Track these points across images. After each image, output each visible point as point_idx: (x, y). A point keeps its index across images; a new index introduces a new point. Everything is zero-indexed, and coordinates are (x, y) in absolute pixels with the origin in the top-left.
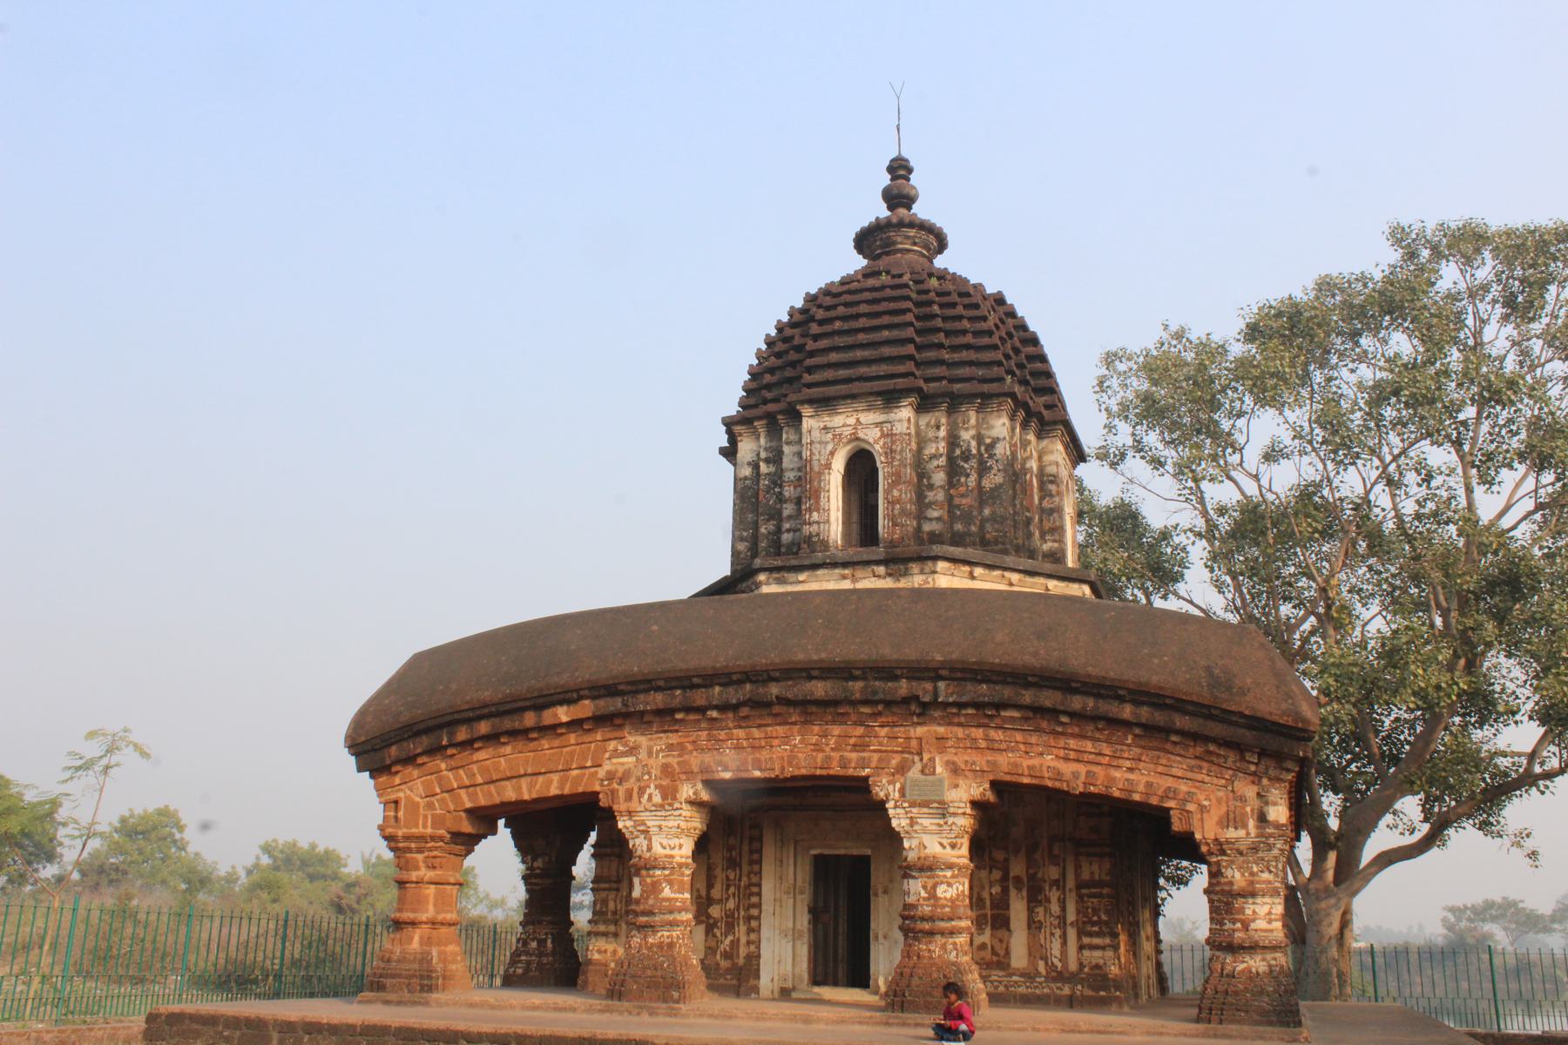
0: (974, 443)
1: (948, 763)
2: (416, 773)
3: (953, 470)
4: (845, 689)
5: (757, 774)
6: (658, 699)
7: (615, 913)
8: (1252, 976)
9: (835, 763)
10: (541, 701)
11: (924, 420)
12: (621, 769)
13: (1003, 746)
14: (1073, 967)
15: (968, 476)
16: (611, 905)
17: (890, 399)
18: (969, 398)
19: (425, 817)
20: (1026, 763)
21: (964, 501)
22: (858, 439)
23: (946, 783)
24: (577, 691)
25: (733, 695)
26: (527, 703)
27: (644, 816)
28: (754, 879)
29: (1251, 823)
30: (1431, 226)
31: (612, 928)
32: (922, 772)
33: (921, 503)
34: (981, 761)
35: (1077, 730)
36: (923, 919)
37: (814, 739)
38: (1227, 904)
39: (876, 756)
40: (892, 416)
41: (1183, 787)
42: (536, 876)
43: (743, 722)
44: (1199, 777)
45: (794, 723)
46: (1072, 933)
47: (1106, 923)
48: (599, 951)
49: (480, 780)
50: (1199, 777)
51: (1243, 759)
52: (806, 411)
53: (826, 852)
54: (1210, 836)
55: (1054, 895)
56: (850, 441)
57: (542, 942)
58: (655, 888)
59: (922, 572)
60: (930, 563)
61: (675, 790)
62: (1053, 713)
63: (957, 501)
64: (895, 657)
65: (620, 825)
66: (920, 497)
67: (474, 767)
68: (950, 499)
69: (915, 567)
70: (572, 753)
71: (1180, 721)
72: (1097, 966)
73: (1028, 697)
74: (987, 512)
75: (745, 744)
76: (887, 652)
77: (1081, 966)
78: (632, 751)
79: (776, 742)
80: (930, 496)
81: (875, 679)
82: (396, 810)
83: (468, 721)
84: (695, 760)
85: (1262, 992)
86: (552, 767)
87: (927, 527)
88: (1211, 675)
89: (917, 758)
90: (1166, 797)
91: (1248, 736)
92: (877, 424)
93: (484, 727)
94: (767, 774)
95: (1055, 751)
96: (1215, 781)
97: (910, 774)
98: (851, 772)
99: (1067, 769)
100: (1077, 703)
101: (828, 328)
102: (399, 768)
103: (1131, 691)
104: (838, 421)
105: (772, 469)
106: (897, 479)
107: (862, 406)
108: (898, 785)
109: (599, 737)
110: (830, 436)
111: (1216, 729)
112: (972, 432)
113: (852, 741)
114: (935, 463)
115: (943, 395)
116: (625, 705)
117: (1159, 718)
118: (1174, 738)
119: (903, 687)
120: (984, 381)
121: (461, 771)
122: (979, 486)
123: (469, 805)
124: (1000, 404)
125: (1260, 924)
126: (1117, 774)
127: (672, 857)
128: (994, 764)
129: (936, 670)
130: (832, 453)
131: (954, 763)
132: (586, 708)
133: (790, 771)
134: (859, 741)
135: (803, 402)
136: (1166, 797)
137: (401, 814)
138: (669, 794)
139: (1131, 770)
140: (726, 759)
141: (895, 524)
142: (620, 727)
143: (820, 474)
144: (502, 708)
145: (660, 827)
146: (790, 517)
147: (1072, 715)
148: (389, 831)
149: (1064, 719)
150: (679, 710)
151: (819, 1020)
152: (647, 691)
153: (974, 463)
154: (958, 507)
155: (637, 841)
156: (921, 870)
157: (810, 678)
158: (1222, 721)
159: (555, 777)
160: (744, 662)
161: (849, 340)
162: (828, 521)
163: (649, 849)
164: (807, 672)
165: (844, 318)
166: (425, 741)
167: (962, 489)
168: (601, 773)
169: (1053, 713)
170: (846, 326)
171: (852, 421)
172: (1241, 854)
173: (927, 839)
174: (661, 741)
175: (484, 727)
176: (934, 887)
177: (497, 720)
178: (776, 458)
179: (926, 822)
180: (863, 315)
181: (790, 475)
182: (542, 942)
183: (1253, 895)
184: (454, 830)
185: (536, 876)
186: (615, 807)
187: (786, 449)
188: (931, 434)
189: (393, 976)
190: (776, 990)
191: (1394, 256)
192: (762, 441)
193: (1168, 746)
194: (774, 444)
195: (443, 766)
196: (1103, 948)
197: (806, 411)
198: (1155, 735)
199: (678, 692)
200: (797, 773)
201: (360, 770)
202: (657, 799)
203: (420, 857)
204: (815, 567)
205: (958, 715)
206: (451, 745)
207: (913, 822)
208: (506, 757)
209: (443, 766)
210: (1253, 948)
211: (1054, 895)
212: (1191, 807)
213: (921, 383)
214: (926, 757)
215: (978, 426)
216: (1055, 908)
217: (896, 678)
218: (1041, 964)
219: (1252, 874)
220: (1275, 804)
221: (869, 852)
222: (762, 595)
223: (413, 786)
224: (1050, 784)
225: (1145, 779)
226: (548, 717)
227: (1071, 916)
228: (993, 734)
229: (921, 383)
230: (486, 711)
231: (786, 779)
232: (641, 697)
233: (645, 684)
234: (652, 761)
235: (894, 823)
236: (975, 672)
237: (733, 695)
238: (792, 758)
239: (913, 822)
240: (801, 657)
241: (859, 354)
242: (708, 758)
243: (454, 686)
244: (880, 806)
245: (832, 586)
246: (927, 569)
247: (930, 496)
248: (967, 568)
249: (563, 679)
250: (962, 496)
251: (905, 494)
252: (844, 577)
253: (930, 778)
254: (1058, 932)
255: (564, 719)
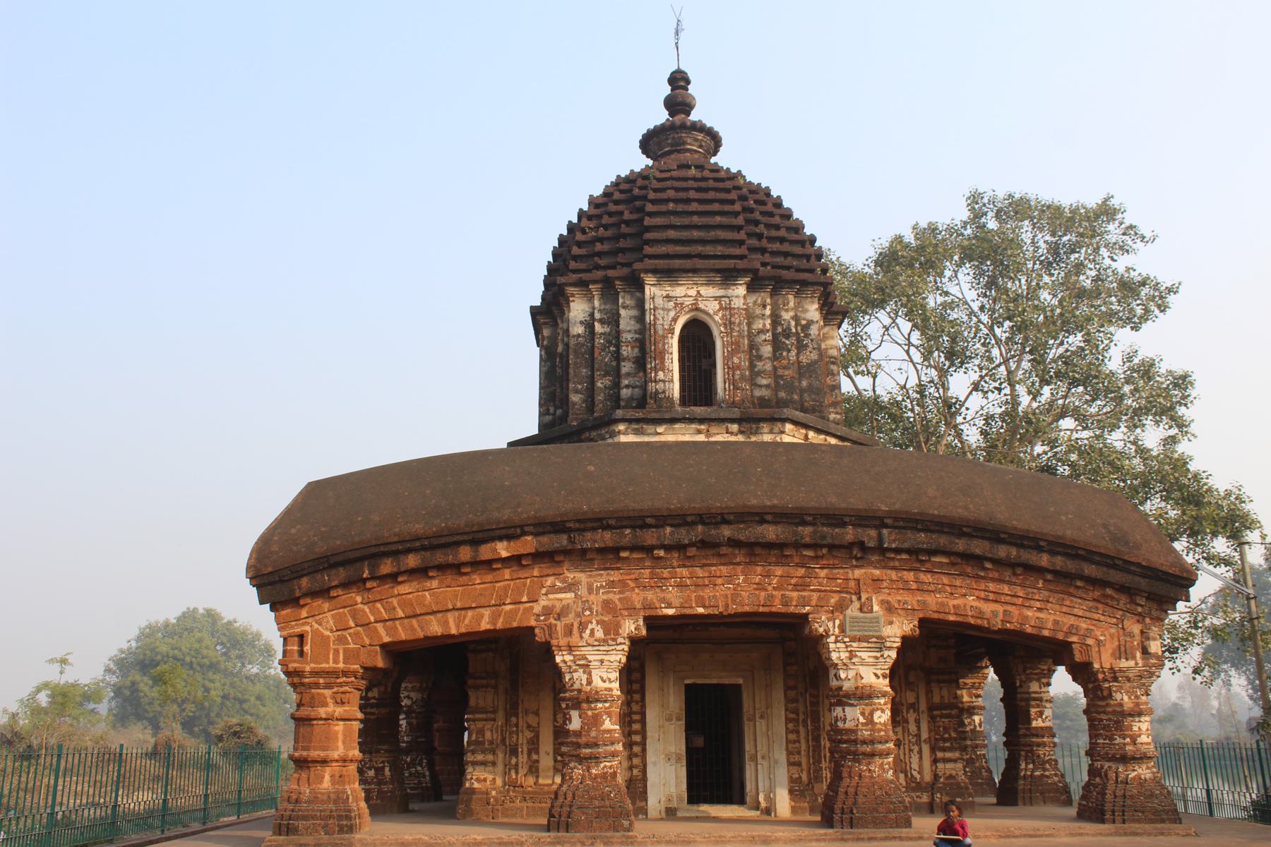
0: (793, 323)
1: (882, 602)
2: (326, 606)
3: (777, 344)
4: (795, 533)
5: (701, 610)
6: (607, 538)
7: (491, 742)
8: (1141, 782)
9: (777, 602)
10: (480, 535)
11: (751, 300)
12: (558, 606)
13: (932, 587)
14: (928, 777)
15: (789, 351)
16: (488, 735)
17: (728, 277)
18: (791, 283)
19: (337, 651)
20: (952, 603)
21: (787, 373)
22: (697, 309)
23: (882, 620)
24: (521, 527)
25: (684, 535)
26: (465, 537)
27: (586, 651)
28: (635, 708)
29: (1138, 655)
30: (1001, 194)
31: (490, 757)
32: (861, 610)
33: (755, 374)
34: (912, 600)
35: (996, 575)
36: (864, 742)
37: (757, 579)
38: (1117, 722)
39: (815, 596)
40: (730, 292)
41: (1084, 626)
42: (372, 706)
43: (687, 561)
44: (1096, 616)
45: (739, 564)
46: (926, 749)
47: (955, 739)
48: (478, 780)
49: (401, 614)
50: (1096, 616)
51: (1133, 602)
52: (649, 280)
53: (700, 681)
54: (1107, 665)
55: (912, 717)
56: (691, 310)
57: (379, 771)
58: (596, 720)
59: (771, 432)
60: (779, 425)
61: (618, 626)
62: (977, 560)
63: (780, 372)
64: (843, 505)
65: (558, 659)
66: (752, 366)
67: (395, 601)
68: (775, 368)
69: (765, 427)
70: (506, 588)
71: (1089, 570)
72: (951, 777)
73: (961, 545)
74: (804, 383)
75: (688, 582)
76: (832, 500)
77: (936, 777)
78: (571, 587)
79: (719, 581)
80: (760, 365)
81: (823, 525)
82: (301, 644)
83: (395, 554)
84: (637, 597)
85: (1152, 795)
86: (483, 601)
87: (758, 393)
88: (1109, 531)
89: (854, 598)
90: (1069, 633)
91: (1143, 583)
92: (716, 298)
93: (412, 561)
94: (710, 611)
95: (977, 593)
96: (1109, 620)
97: (849, 612)
98: (792, 609)
99: (987, 608)
100: (1002, 551)
101: (663, 208)
102: (308, 600)
103: (1050, 543)
104: (679, 291)
105: (607, 329)
106: (735, 348)
107: (701, 280)
108: (837, 622)
109: (536, 573)
110: (672, 304)
111: (1116, 576)
112: (792, 314)
113: (793, 581)
114: (763, 337)
115: (770, 278)
116: (571, 541)
117: (1071, 566)
118: (1079, 583)
119: (849, 534)
120: (798, 270)
121: (378, 605)
122: (799, 362)
123: (387, 639)
124: (814, 292)
125: (1144, 739)
126: (1030, 613)
127: (611, 690)
128: (924, 603)
129: (881, 519)
130: (675, 320)
131: (888, 602)
132: (528, 544)
133: (734, 608)
134: (800, 581)
135: (647, 271)
136: (1069, 633)
137: (307, 648)
138: (611, 630)
139: (1040, 610)
140: (669, 596)
141: (736, 388)
142: (559, 563)
143: (664, 337)
144: (435, 542)
145: (602, 661)
146: (628, 374)
147: (996, 562)
148: (292, 666)
149: (988, 565)
150: (624, 549)
151: (777, 840)
152: (594, 529)
153: (793, 340)
154: (781, 377)
155: (576, 675)
156: (861, 698)
157: (763, 521)
158: (1121, 570)
159: (487, 613)
160: (697, 505)
161: (686, 221)
162: (672, 381)
163: (589, 682)
164: (760, 517)
165: (676, 201)
166: (342, 574)
167: (784, 362)
168: (537, 608)
169: (977, 560)
170: (680, 208)
171: (693, 292)
172: (1129, 680)
173: (863, 671)
174: (601, 579)
175: (412, 561)
176: (871, 714)
177: (428, 554)
178: (613, 319)
179: (864, 655)
180: (695, 200)
181: (627, 337)
182: (379, 771)
183: (1140, 714)
184: (370, 664)
185: (372, 706)
186: (554, 642)
187: (623, 312)
188: (758, 311)
189: (305, 818)
190: (663, 809)
191: (965, 214)
192: (597, 303)
193: (1072, 590)
194: (608, 307)
195: (359, 599)
196: (955, 761)
197: (649, 280)
198: (1063, 578)
199: (628, 531)
200: (740, 610)
201: (262, 602)
202: (600, 634)
203: (327, 692)
204: (673, 421)
205: (893, 559)
206: (373, 578)
207: (852, 655)
208: (433, 591)
209: (359, 599)
210: (1142, 758)
211: (912, 717)
212: (1090, 641)
213: (758, 266)
214: (864, 596)
215: (796, 308)
216: (913, 728)
217: (844, 525)
218: (902, 776)
219: (1137, 697)
220: (1155, 639)
221: (741, 681)
222: (620, 443)
223: (321, 621)
224: (972, 621)
225: (1052, 618)
226: (485, 552)
227: (925, 735)
228: (922, 577)
229: (758, 266)
230: (418, 544)
231: (730, 615)
232: (589, 535)
233: (599, 522)
234: (592, 597)
235: (834, 656)
236: (917, 521)
237: (684, 535)
238: (735, 596)
239: (852, 655)
240: (754, 502)
241: (696, 234)
242: (650, 595)
243: (376, 518)
244: (816, 644)
245: (687, 438)
246: (776, 430)
247: (760, 365)
248: (804, 431)
249: (506, 514)
250: (784, 368)
251: (741, 360)
252: (699, 432)
253: (869, 615)
254: (916, 748)
255: (504, 554)
